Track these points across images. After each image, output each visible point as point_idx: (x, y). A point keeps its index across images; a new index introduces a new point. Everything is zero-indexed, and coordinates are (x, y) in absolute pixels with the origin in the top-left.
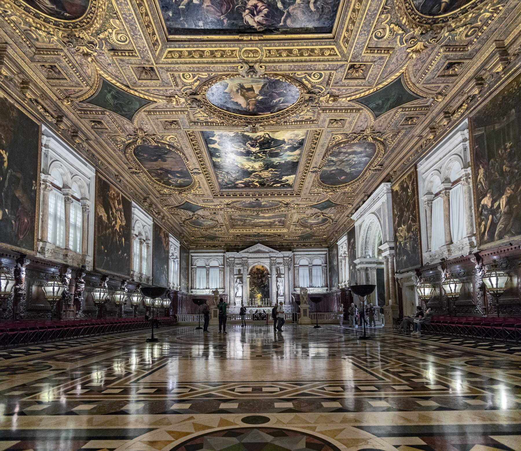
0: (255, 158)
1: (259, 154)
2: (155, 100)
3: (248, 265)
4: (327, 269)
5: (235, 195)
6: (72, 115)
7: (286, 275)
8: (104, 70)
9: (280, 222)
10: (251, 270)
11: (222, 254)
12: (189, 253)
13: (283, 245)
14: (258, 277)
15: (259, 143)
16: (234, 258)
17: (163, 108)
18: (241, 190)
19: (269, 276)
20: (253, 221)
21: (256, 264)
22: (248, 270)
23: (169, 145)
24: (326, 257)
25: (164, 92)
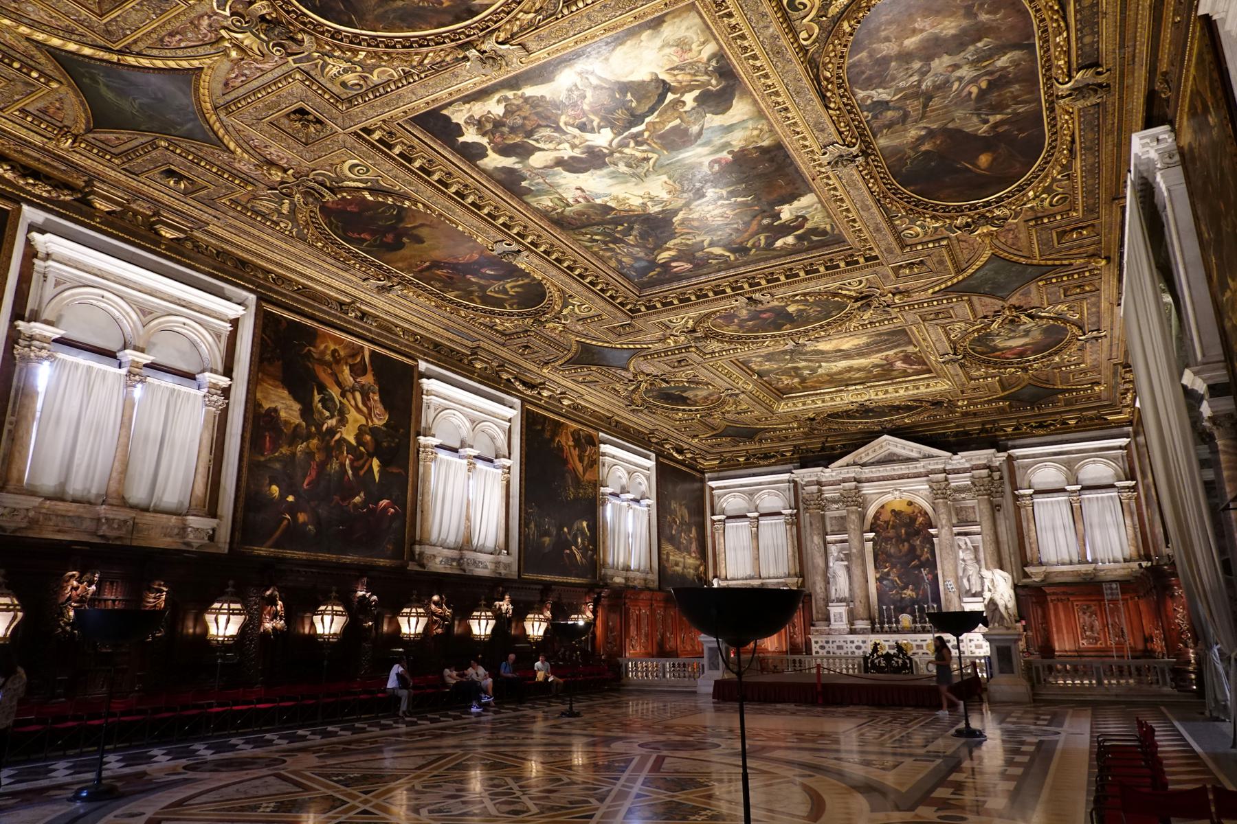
0: (629, 165)
1: (627, 150)
2: (196, 63)
3: (865, 501)
4: (1138, 499)
5: (684, 300)
6: (113, 173)
7: (987, 524)
8: (26, 21)
9: (907, 359)
10: (876, 517)
11: (786, 476)
12: (702, 481)
13: (966, 433)
14: (898, 537)
16: (819, 483)
17: (243, 83)
18: (695, 281)
19: (932, 531)
20: (820, 371)
21: (889, 498)
22: (863, 517)
23: (370, 190)
24: (1129, 455)
25: (195, 32)
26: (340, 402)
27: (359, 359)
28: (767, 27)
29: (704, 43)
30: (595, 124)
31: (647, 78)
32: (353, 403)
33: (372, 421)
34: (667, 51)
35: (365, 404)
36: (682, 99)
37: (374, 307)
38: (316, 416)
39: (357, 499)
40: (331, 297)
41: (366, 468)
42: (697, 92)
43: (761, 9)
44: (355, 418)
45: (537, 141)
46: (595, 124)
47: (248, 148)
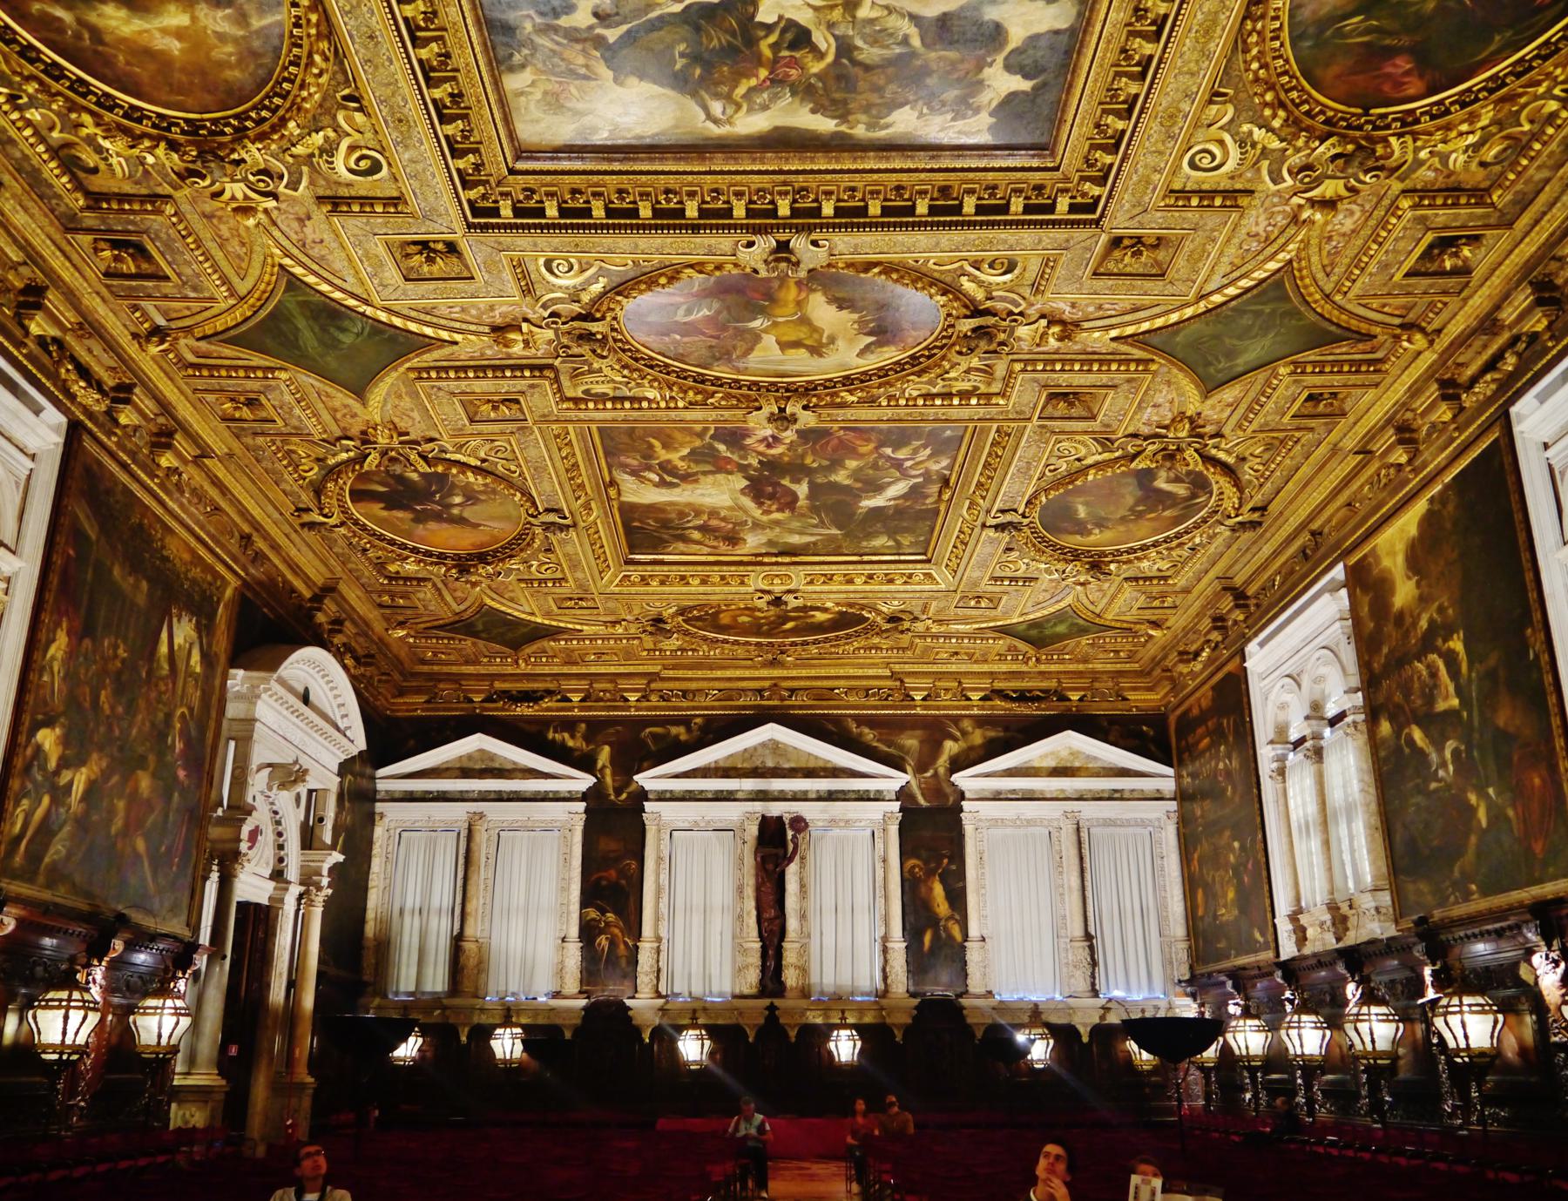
15: (759, 60)
28: (412, 161)
29: (522, 93)
30: (773, 39)
31: (633, 81)
34: (580, 106)
36: (594, 21)
42: (564, 21)
43: (415, 184)
45: (905, 41)
46: (773, 39)
47: (1281, 241)
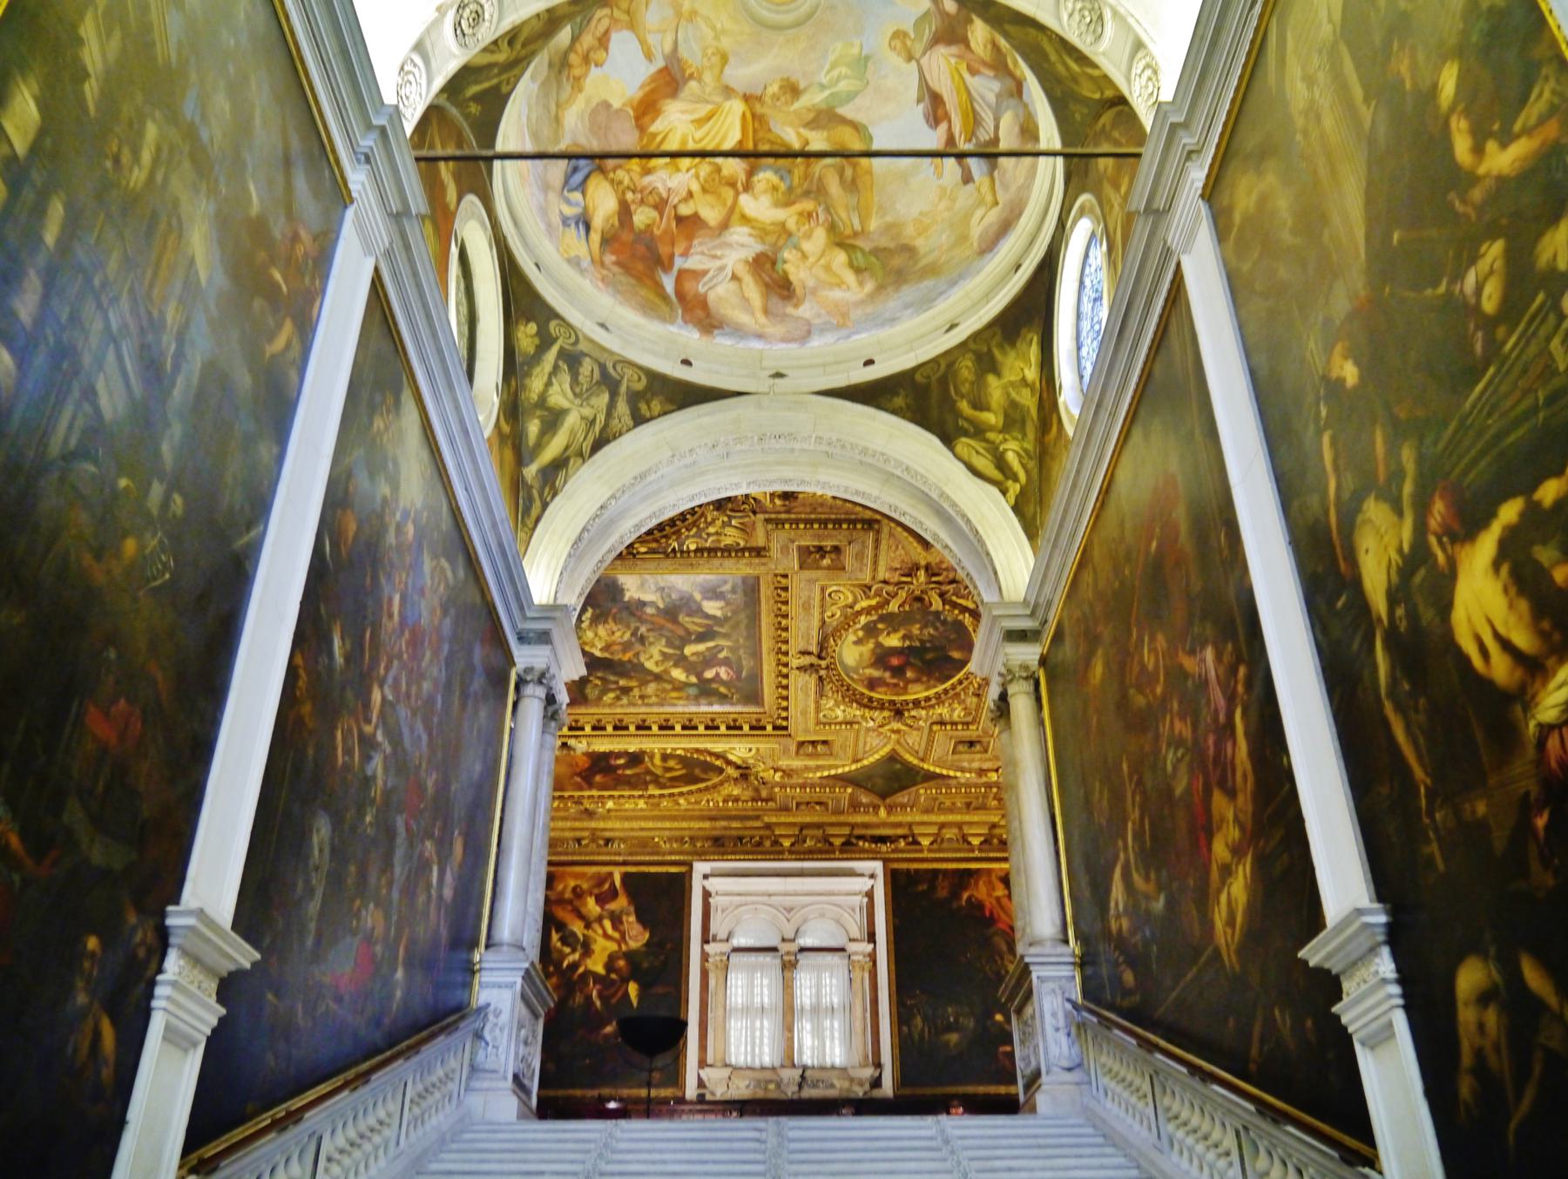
26: (584, 935)
27: (607, 886)
32: (600, 931)
33: (626, 943)
35: (615, 927)
37: (611, 830)
38: (555, 955)
39: (609, 1029)
40: (567, 840)
41: (620, 994)
44: (603, 948)
